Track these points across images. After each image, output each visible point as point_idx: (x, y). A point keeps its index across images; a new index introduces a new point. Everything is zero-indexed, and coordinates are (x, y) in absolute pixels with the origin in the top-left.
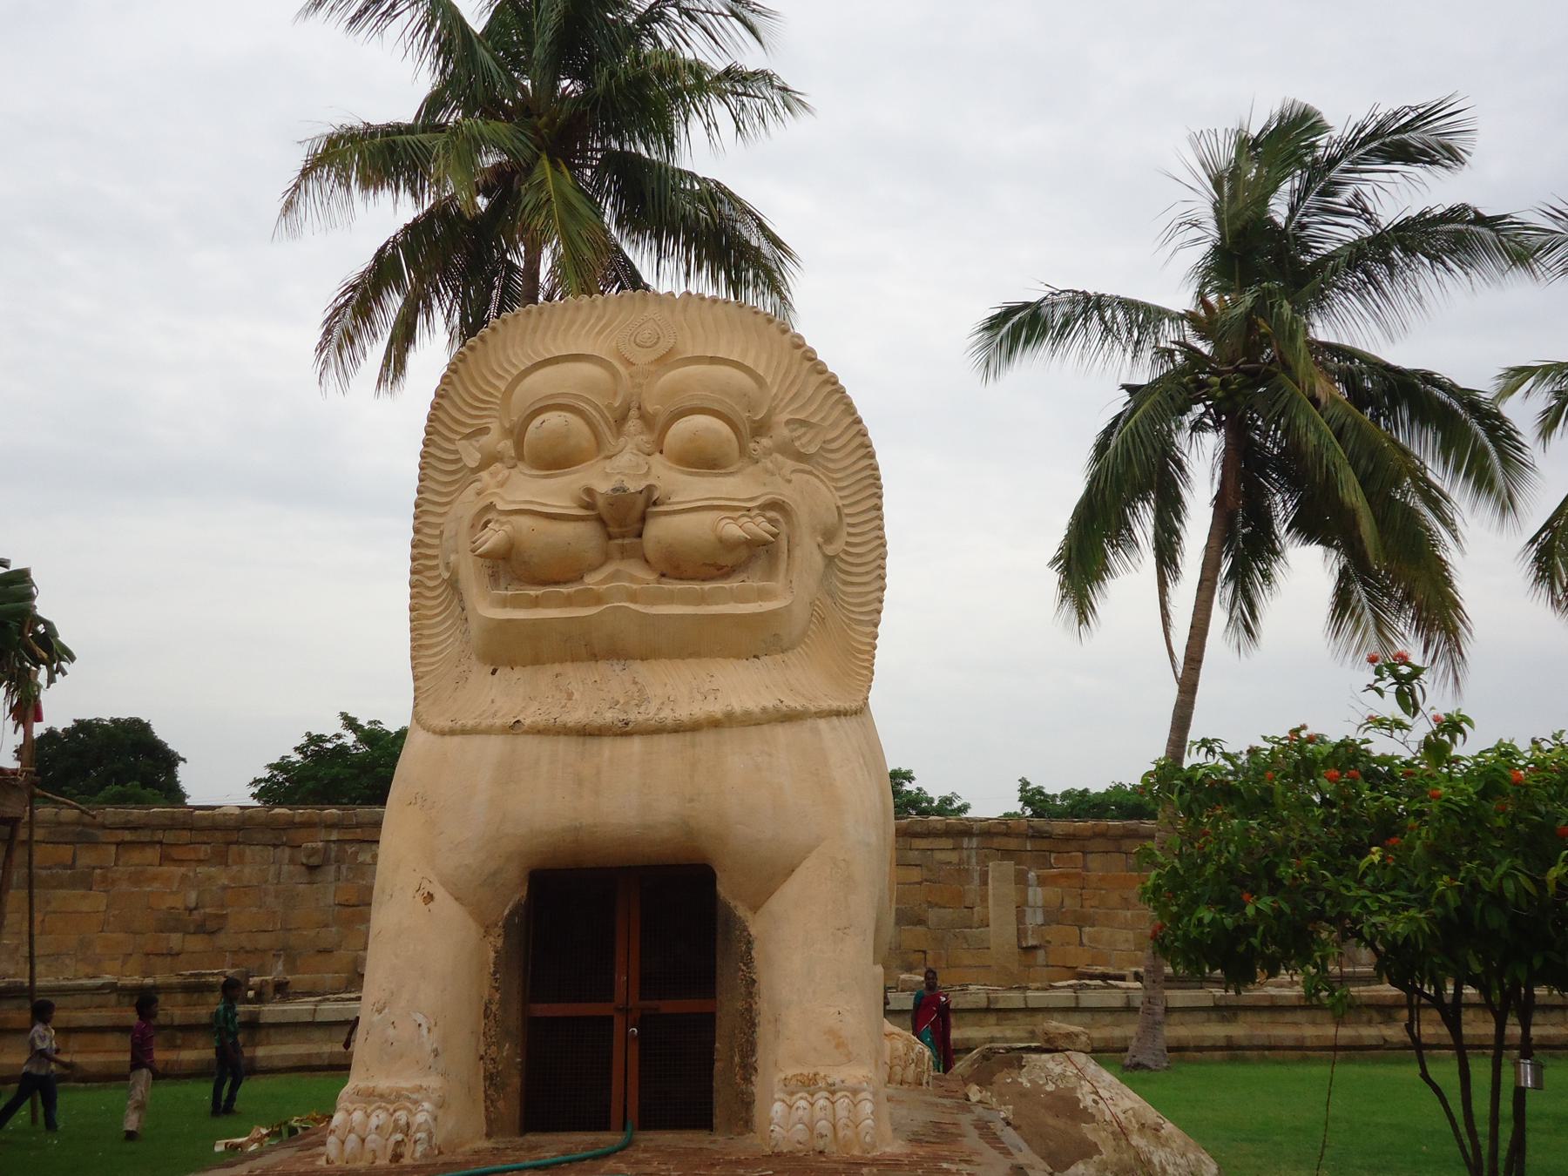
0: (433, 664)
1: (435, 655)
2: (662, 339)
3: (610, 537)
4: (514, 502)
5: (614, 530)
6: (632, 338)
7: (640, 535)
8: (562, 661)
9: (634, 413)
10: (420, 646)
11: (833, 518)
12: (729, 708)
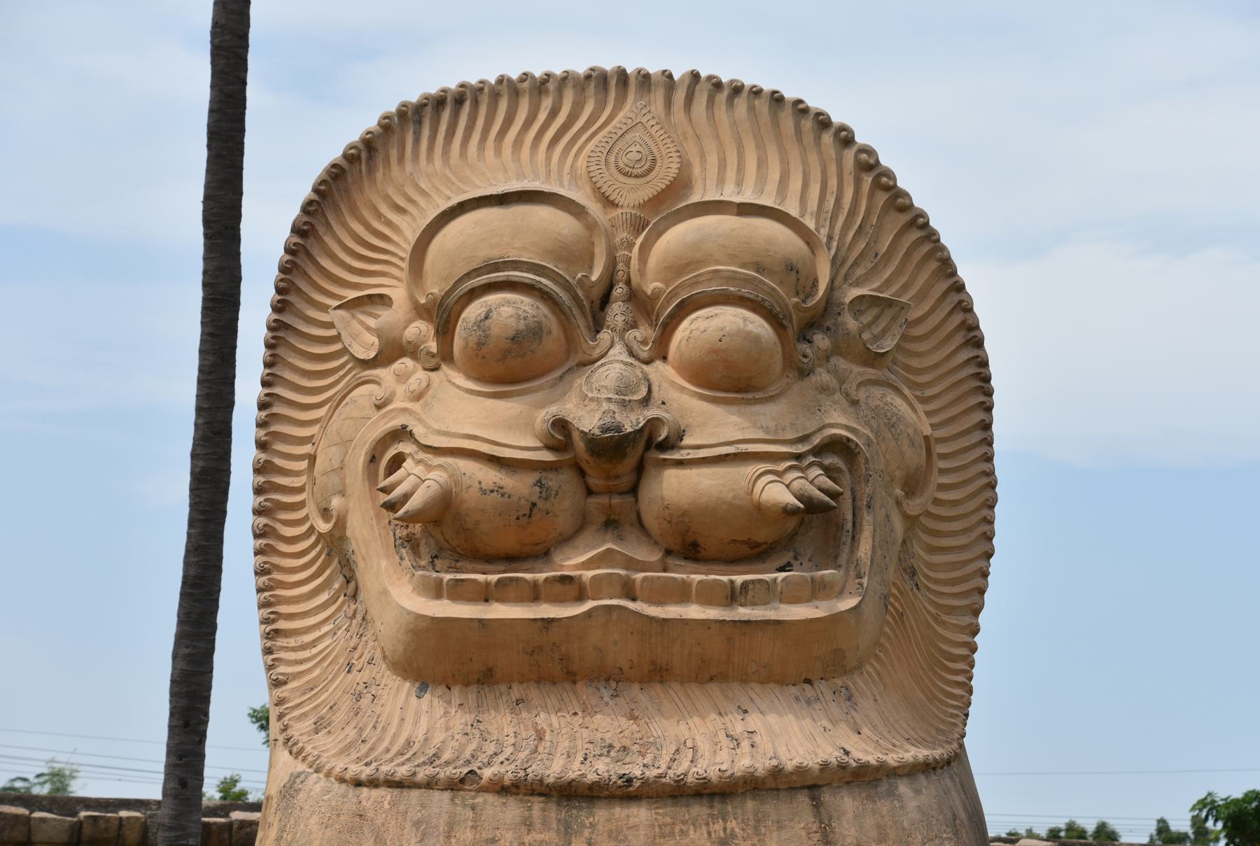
0: (300, 662)
1: (303, 647)
2: (659, 164)
3: (590, 492)
4: (446, 434)
5: (595, 481)
6: (612, 159)
7: (634, 490)
8: (523, 681)
9: (619, 290)
10: (277, 631)
11: (915, 457)
12: (774, 762)
